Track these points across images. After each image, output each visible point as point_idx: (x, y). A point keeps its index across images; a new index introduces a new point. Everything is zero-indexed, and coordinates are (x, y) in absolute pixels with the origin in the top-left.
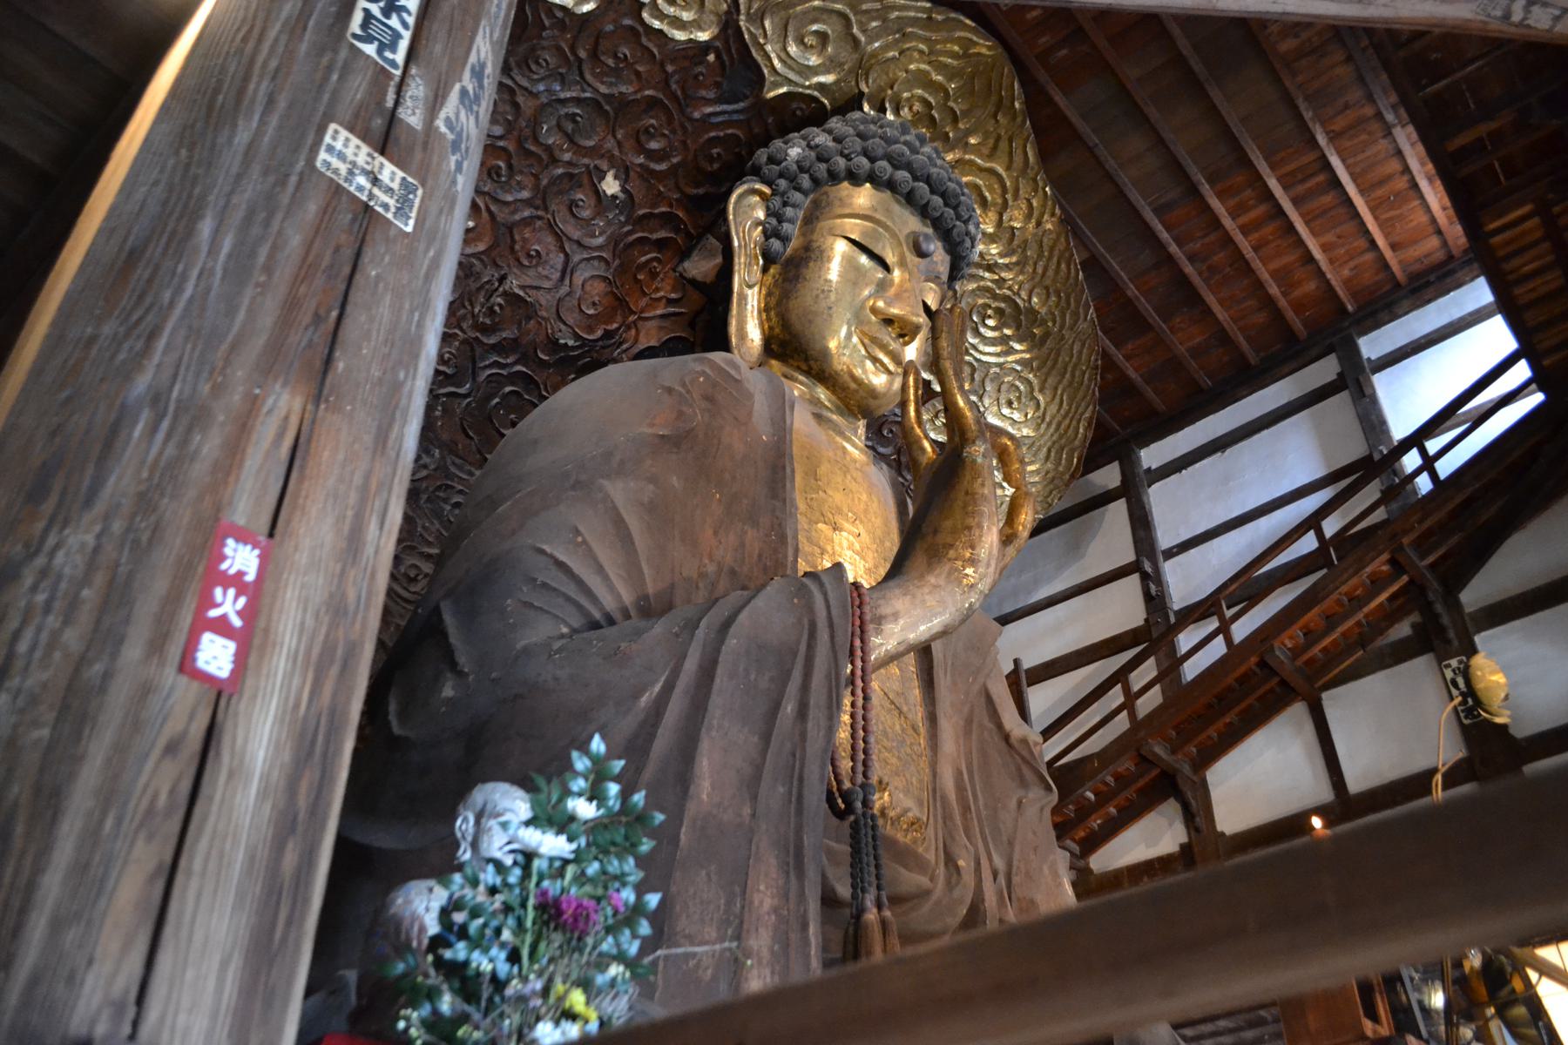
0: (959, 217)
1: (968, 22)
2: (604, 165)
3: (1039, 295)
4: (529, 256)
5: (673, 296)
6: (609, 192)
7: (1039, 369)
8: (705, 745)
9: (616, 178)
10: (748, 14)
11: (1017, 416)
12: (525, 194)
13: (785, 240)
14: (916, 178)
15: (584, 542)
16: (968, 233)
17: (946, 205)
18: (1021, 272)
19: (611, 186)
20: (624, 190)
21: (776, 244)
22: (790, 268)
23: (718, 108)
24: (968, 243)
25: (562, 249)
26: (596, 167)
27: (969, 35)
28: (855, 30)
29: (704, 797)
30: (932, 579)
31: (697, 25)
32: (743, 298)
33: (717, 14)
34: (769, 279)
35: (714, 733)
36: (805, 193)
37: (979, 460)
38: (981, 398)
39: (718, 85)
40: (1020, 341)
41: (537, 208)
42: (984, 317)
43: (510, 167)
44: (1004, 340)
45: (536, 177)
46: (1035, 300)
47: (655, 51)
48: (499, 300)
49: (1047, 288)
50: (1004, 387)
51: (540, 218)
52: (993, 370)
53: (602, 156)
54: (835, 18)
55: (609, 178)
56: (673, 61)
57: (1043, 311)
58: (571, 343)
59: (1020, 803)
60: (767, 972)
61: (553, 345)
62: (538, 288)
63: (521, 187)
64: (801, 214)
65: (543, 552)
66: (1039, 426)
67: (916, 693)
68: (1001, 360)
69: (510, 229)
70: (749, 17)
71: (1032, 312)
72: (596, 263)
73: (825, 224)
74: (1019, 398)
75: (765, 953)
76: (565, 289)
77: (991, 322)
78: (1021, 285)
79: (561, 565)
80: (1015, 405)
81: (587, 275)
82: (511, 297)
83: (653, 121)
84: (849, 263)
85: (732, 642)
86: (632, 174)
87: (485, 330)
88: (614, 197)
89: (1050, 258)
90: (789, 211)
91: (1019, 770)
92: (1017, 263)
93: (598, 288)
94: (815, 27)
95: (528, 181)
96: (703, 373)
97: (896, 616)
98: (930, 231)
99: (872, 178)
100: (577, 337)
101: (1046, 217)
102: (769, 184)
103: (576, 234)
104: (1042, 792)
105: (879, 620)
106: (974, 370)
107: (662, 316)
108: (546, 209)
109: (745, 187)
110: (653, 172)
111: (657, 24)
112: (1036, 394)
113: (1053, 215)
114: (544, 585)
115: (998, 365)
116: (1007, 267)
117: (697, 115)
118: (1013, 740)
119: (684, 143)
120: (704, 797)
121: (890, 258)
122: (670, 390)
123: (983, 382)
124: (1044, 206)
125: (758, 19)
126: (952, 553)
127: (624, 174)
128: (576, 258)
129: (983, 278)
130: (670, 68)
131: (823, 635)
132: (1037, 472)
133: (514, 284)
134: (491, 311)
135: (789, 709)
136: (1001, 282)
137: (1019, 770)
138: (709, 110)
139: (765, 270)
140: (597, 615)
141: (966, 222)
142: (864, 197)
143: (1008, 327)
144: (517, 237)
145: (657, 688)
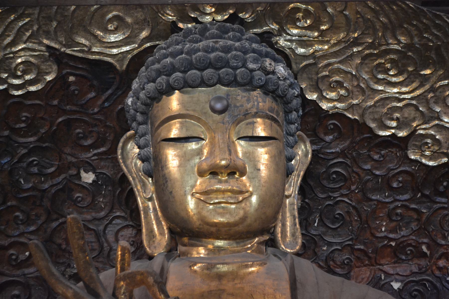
0: (235, 68)
3: (402, 34)
6: (90, 181)
9: (86, 171)
10: (65, 46)
12: (43, 218)
14: (184, 72)
16: (252, 71)
19: (88, 178)
23: (103, 98)
26: (71, 176)
31: (41, 74)
32: (146, 209)
39: (92, 87)
40: (425, 69)
41: (57, 219)
43: (22, 211)
47: (38, 102)
53: (69, 168)
55: (83, 174)
56: (53, 98)
57: (416, 40)
63: (38, 216)
68: (427, 87)
71: (409, 47)
72: (118, 221)
77: (391, 73)
78: (383, 36)
83: (78, 131)
94: (110, 16)
98: (222, 90)
109: (122, 140)
111: (20, 93)
115: (428, 91)
117: (96, 110)
119: (106, 126)
123: (430, 109)
125: (72, 43)
128: (101, 228)
130: (55, 102)
136: (371, 46)
138: (99, 102)
142: (174, 102)
144: (60, 241)
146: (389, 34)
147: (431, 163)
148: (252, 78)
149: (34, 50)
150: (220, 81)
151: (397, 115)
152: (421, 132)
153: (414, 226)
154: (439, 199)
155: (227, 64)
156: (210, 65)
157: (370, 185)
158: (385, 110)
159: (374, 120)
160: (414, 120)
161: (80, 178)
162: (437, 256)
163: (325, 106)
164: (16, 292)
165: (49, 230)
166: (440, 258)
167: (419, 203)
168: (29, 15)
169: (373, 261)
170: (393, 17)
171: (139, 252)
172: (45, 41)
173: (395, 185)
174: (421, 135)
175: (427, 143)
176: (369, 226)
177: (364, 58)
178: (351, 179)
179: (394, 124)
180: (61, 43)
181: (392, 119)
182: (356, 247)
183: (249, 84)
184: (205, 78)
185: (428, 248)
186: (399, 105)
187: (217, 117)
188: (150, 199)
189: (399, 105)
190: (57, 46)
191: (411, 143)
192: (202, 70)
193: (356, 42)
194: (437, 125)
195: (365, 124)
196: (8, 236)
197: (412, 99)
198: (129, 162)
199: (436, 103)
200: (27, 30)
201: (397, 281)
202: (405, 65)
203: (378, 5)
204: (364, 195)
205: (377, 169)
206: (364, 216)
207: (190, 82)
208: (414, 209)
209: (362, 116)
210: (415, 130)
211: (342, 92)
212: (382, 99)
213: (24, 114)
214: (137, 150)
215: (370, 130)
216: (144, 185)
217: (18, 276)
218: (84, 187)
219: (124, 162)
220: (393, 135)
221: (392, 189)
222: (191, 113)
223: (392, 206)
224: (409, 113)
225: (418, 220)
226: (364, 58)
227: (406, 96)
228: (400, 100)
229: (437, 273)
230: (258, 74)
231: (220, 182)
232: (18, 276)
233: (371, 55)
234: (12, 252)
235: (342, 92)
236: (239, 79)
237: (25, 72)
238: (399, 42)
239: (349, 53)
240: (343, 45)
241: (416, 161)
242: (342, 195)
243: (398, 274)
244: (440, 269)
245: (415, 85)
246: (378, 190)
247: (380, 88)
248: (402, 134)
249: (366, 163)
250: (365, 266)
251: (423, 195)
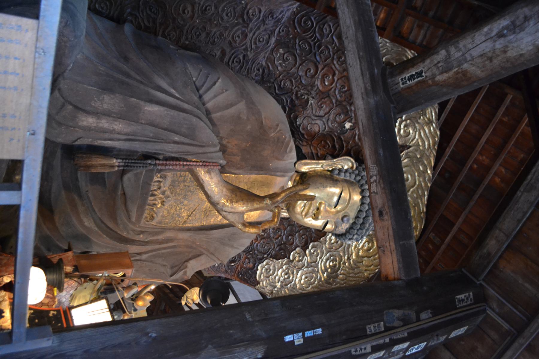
0: (358, 230)
1: (423, 225)
2: (353, 121)
3: (343, 277)
4: (321, 104)
5: (319, 155)
6: (346, 125)
7: (319, 285)
8: (162, 109)
9: (351, 126)
10: (408, 152)
11: (302, 281)
12: (339, 98)
13: (339, 174)
14: (366, 212)
15: (223, 92)
16: (354, 235)
17: (361, 225)
18: (349, 269)
19: (348, 125)
20: (347, 130)
21: (337, 172)
22: (331, 178)
24: (351, 237)
25: (326, 114)
26: (352, 119)
27: (419, 227)
28: (412, 189)
29: (146, 108)
30: (224, 190)
31: (401, 137)
32: (318, 164)
33: (405, 142)
34: (325, 172)
35: (166, 112)
36: (355, 179)
37: (265, 202)
38: (307, 267)
40: (327, 275)
41: (336, 103)
42: (333, 261)
43: (346, 91)
44: (326, 270)
45: (345, 100)
46: (341, 276)
48: (306, 97)
49: (346, 279)
50: (311, 274)
51: (333, 105)
52: (316, 269)
54: (413, 182)
55: (350, 124)
57: (338, 280)
58: (298, 123)
59: (165, 266)
60: (95, 125)
61: (296, 117)
62: (312, 109)
63: (341, 96)
64: (348, 178)
65: (218, 79)
66: (301, 289)
67: (197, 224)
68: (320, 271)
69: (328, 96)
70: (407, 154)
71: (337, 276)
72: (324, 126)
73: (345, 185)
74: (308, 280)
75: (101, 125)
76: (314, 118)
77: (331, 264)
78: (345, 270)
79: (215, 83)
80: (306, 280)
81: (320, 125)
82: (307, 101)
84: (333, 194)
85: (194, 119)
86: (353, 131)
87: (297, 94)
88: (345, 127)
89: (355, 277)
90: (348, 174)
91: (176, 266)
92: (352, 267)
93: (317, 129)
94: (409, 176)
95: (343, 99)
96: (286, 138)
97: (211, 178)
98: (351, 221)
99: (363, 197)
100: (300, 125)
101: (368, 272)
102: (357, 168)
103: (331, 117)
104: (170, 274)
105: (209, 172)
106: (315, 262)
107: (312, 153)
108: (336, 106)
109: (354, 161)
110: (355, 137)
112: (311, 286)
113: (369, 274)
114: (207, 77)
116: (350, 264)
118: (186, 263)
120: (146, 108)
121: (339, 208)
122: (277, 125)
123: (312, 266)
124: (372, 270)
126: (234, 196)
127: (352, 129)
128: (324, 120)
129: (345, 257)
131: (201, 150)
132: (285, 292)
133: (311, 101)
134: (302, 95)
135: (176, 138)
136: (344, 263)
137: (176, 266)
139: (328, 171)
140: (201, 92)
141: (357, 234)
142: (357, 198)
143: (331, 270)
144: (326, 99)
145: (177, 95)
146: (345, 272)
147: (292, 254)
148: (351, 234)
149: (412, 141)
150: (354, 223)
151: (315, 253)
153: (272, 235)
154: (278, 248)
156: (363, 223)
157: (294, 229)
158: (319, 251)
159: (317, 245)
160: (310, 258)
161: (349, 122)
164: (312, 71)
165: (332, 98)
168: (428, 149)
170: (351, 279)
171: (301, 156)
172: (413, 147)
173: (290, 237)
175: (300, 257)
177: (341, 257)
179: (312, 251)
180: (409, 152)
181: (314, 252)
184: (359, 219)
186: (318, 257)
187: (340, 217)
188: (322, 167)
190: (409, 150)
191: (303, 252)
193: (349, 259)
194: (304, 265)
195: (317, 241)
196: (338, 80)
197: (318, 263)
198: (343, 161)
199: (313, 270)
200: (422, 144)
202: (331, 269)
203: (358, 277)
204: (291, 225)
205: (299, 234)
207: (360, 213)
208: (278, 238)
209: (321, 242)
211: (333, 241)
212: (323, 253)
214: (346, 167)
215: (314, 241)
216: (328, 165)
217: (319, 75)
218: (345, 121)
219: (344, 159)
220: (308, 248)
221: (290, 235)
222: (350, 205)
223: (283, 231)
224: (314, 259)
226: (341, 257)
227: (320, 262)
228: (320, 258)
231: (313, 210)
232: (319, 75)
234: (331, 77)
235: (333, 241)
236: (353, 230)
237: (405, 131)
238: (341, 274)
239: (346, 253)
240: (350, 253)
241: (295, 249)
246: (291, 230)
247: (328, 255)
249: (303, 232)
251: (282, 244)
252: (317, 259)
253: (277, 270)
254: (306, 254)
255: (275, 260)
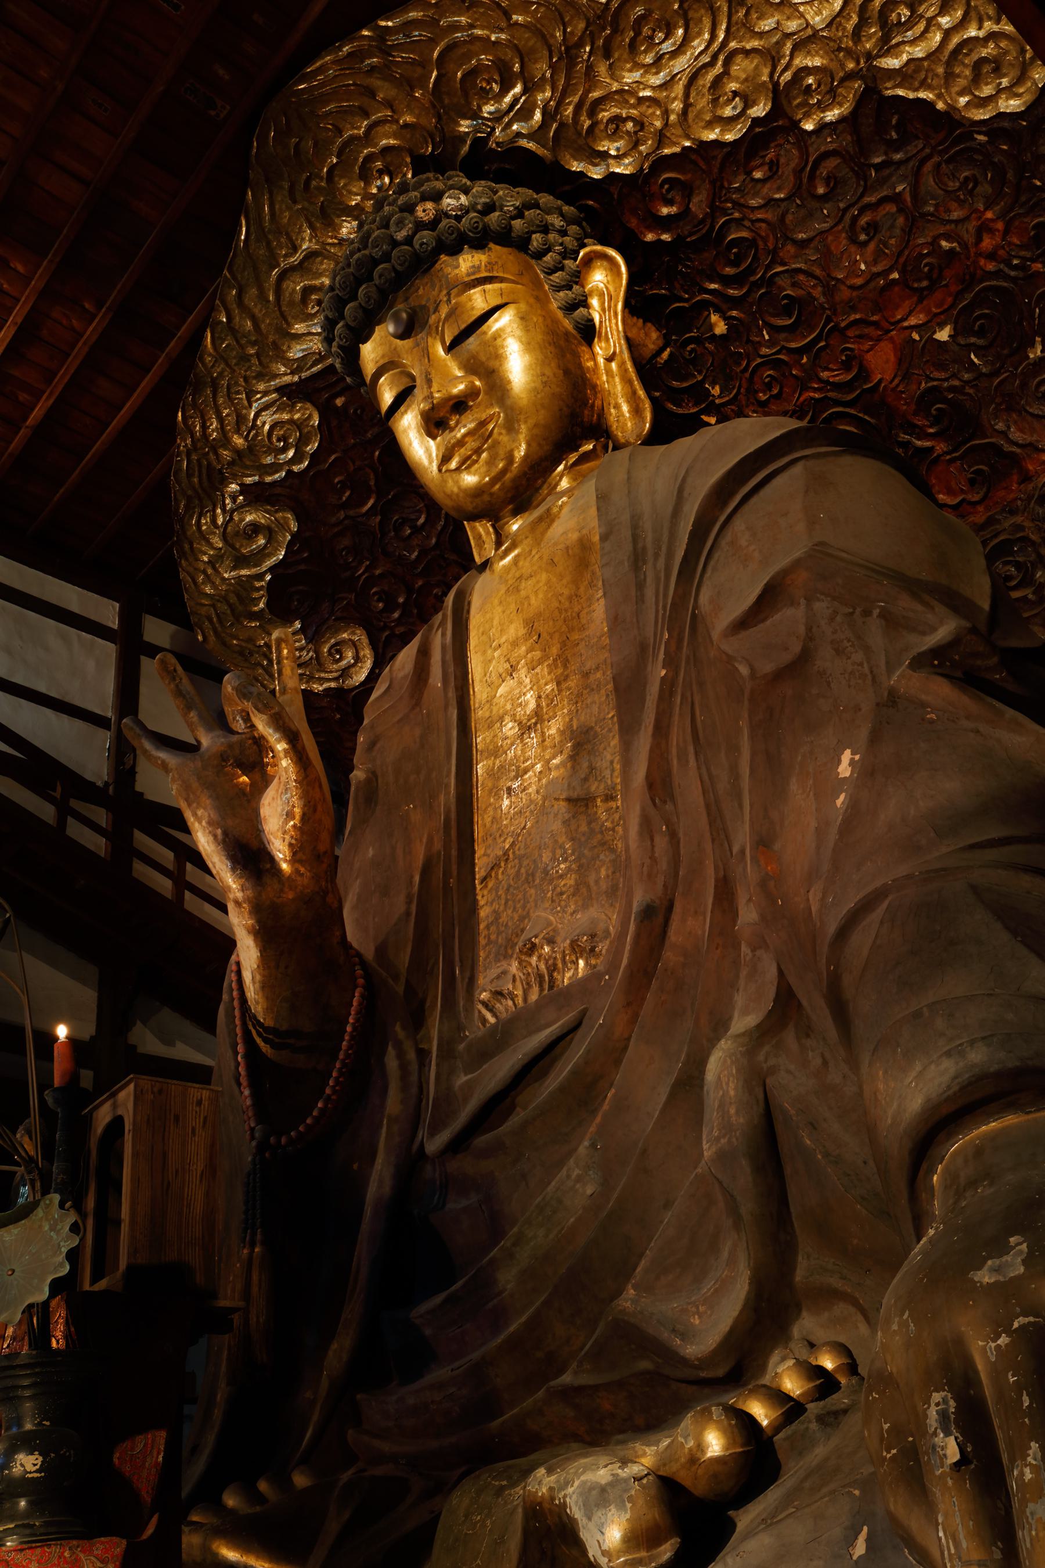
141: (395, 244)
152: (788, 76)
155: (375, 262)
159: (710, 125)
162: (971, 240)
163: (624, 168)
166: (979, 239)
167: (882, 182)
169: (885, 325)
173: (821, 191)
174: (789, 84)
176: (838, 280)
178: (759, 235)
182: (843, 325)
183: (422, 264)
185: (948, 237)
186: (718, 69)
189: (718, 69)
192: (354, 297)
201: (942, 326)
206: (818, 272)
210: (776, 84)
213: (336, 480)
225: (900, 210)
229: (991, 267)
230: (425, 237)
233: (608, 40)
241: (823, 127)
242: (769, 267)
243: (936, 315)
244: (992, 256)
245: (707, 23)
248: (759, 110)
250: (879, 340)
252: (727, 63)
253: (946, 53)
254: (778, 95)
255: (940, 105)
